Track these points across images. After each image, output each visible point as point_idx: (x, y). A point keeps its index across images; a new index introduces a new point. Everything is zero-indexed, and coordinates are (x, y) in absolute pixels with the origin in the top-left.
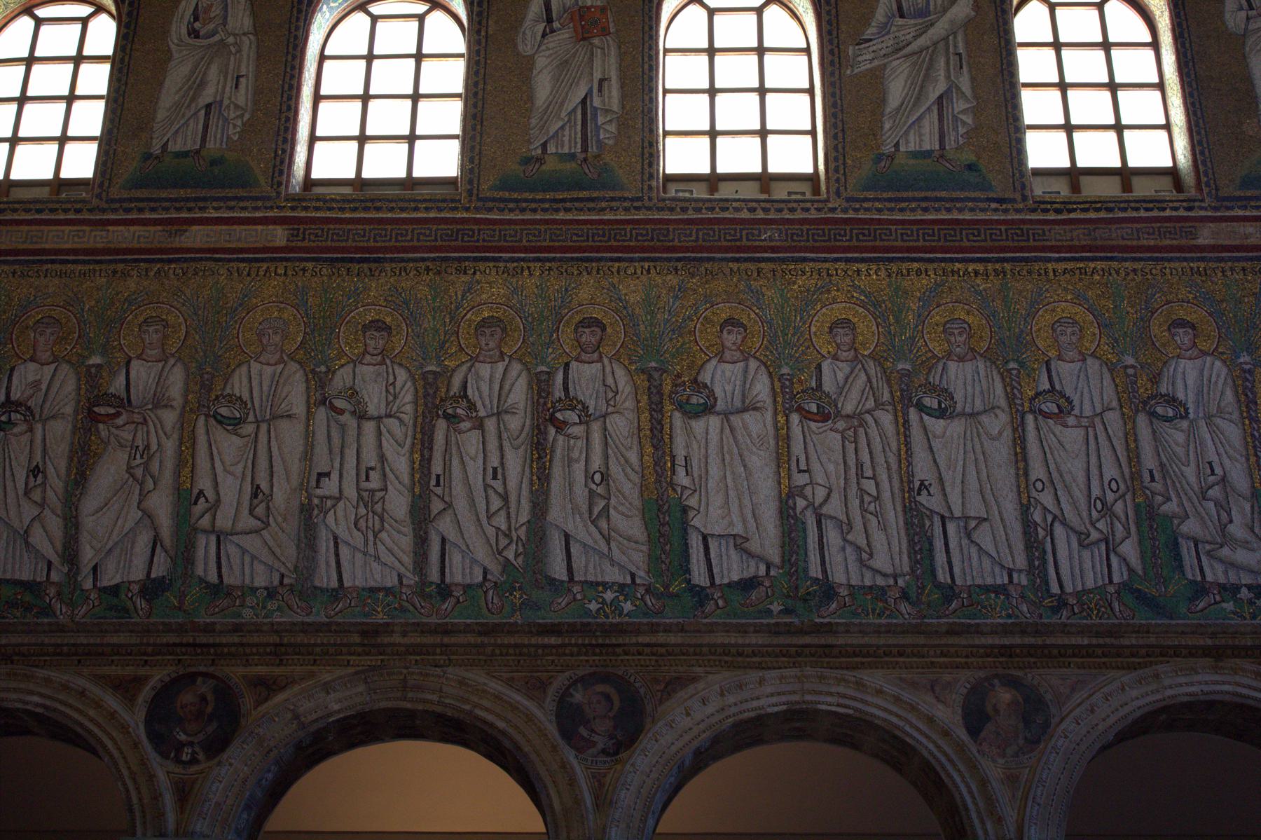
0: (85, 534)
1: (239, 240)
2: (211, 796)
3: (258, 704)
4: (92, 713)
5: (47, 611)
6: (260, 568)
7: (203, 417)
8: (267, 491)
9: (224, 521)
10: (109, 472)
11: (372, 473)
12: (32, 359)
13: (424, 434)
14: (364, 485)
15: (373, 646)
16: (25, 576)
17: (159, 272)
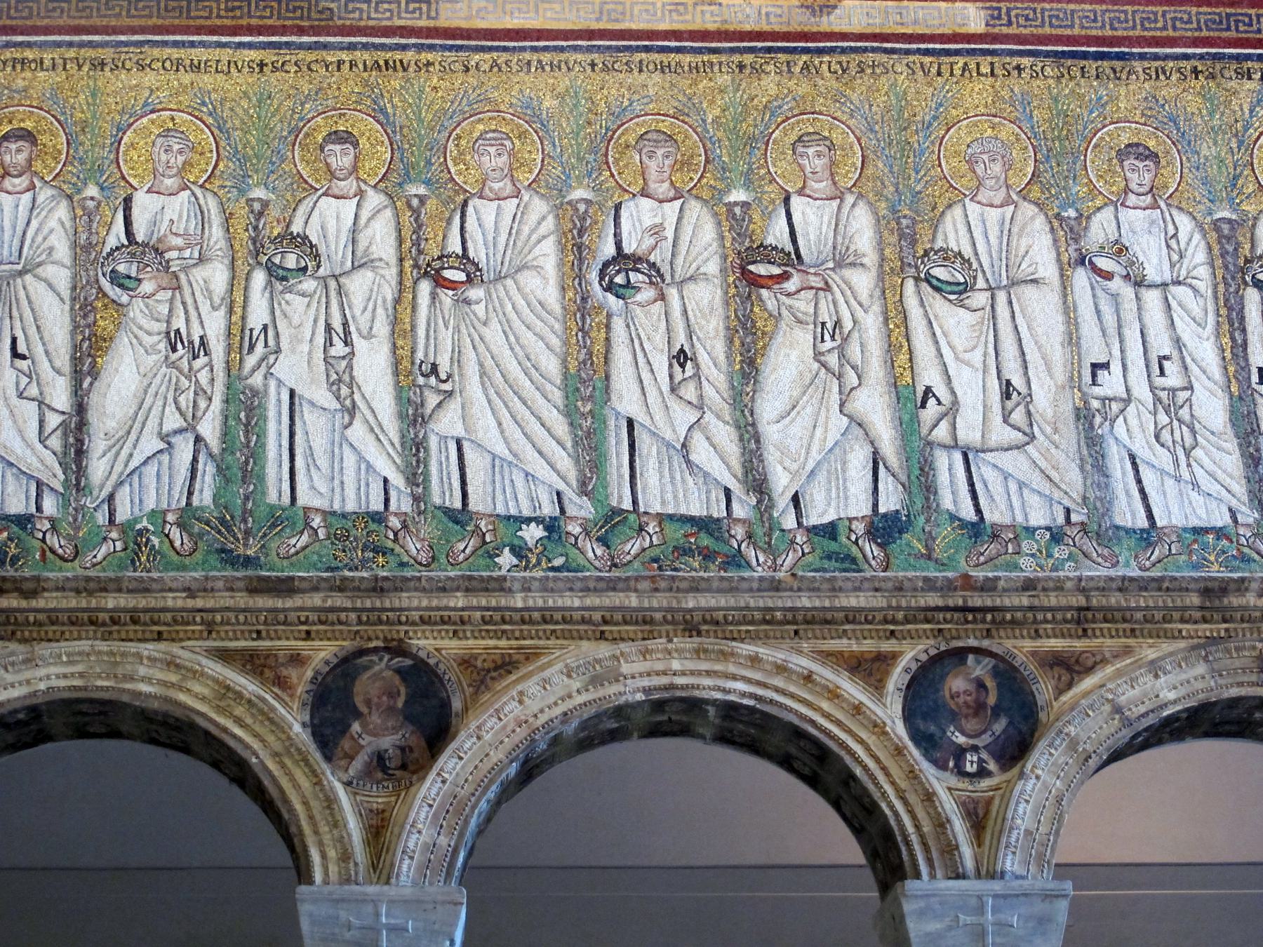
0: (771, 449)
1: (916, 22)
2: (1019, 821)
3: (1060, 692)
4: (825, 705)
5: (736, 560)
6: (1033, 500)
7: (910, 285)
8: (1024, 390)
9: (969, 432)
10: (789, 359)
11: (1166, 364)
12: (645, 193)
13: (1230, 309)
14: (1159, 382)
15: (1217, 609)
16: (696, 510)
17: (806, 67)
